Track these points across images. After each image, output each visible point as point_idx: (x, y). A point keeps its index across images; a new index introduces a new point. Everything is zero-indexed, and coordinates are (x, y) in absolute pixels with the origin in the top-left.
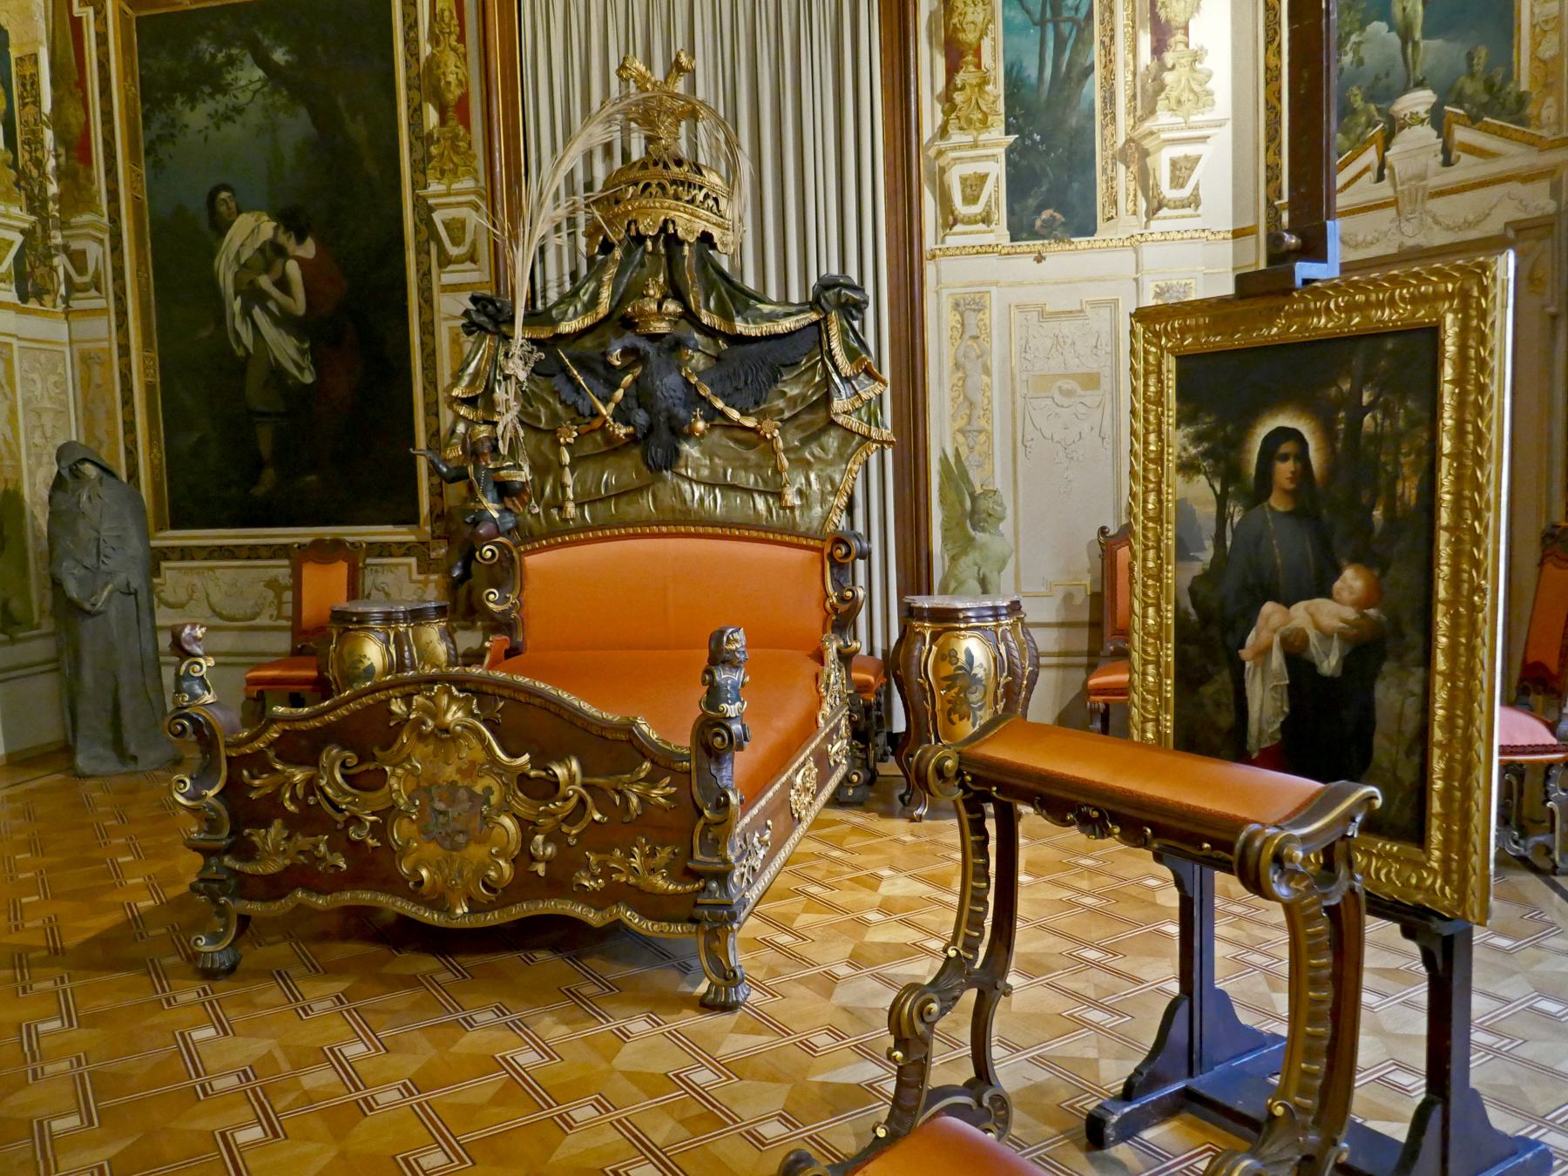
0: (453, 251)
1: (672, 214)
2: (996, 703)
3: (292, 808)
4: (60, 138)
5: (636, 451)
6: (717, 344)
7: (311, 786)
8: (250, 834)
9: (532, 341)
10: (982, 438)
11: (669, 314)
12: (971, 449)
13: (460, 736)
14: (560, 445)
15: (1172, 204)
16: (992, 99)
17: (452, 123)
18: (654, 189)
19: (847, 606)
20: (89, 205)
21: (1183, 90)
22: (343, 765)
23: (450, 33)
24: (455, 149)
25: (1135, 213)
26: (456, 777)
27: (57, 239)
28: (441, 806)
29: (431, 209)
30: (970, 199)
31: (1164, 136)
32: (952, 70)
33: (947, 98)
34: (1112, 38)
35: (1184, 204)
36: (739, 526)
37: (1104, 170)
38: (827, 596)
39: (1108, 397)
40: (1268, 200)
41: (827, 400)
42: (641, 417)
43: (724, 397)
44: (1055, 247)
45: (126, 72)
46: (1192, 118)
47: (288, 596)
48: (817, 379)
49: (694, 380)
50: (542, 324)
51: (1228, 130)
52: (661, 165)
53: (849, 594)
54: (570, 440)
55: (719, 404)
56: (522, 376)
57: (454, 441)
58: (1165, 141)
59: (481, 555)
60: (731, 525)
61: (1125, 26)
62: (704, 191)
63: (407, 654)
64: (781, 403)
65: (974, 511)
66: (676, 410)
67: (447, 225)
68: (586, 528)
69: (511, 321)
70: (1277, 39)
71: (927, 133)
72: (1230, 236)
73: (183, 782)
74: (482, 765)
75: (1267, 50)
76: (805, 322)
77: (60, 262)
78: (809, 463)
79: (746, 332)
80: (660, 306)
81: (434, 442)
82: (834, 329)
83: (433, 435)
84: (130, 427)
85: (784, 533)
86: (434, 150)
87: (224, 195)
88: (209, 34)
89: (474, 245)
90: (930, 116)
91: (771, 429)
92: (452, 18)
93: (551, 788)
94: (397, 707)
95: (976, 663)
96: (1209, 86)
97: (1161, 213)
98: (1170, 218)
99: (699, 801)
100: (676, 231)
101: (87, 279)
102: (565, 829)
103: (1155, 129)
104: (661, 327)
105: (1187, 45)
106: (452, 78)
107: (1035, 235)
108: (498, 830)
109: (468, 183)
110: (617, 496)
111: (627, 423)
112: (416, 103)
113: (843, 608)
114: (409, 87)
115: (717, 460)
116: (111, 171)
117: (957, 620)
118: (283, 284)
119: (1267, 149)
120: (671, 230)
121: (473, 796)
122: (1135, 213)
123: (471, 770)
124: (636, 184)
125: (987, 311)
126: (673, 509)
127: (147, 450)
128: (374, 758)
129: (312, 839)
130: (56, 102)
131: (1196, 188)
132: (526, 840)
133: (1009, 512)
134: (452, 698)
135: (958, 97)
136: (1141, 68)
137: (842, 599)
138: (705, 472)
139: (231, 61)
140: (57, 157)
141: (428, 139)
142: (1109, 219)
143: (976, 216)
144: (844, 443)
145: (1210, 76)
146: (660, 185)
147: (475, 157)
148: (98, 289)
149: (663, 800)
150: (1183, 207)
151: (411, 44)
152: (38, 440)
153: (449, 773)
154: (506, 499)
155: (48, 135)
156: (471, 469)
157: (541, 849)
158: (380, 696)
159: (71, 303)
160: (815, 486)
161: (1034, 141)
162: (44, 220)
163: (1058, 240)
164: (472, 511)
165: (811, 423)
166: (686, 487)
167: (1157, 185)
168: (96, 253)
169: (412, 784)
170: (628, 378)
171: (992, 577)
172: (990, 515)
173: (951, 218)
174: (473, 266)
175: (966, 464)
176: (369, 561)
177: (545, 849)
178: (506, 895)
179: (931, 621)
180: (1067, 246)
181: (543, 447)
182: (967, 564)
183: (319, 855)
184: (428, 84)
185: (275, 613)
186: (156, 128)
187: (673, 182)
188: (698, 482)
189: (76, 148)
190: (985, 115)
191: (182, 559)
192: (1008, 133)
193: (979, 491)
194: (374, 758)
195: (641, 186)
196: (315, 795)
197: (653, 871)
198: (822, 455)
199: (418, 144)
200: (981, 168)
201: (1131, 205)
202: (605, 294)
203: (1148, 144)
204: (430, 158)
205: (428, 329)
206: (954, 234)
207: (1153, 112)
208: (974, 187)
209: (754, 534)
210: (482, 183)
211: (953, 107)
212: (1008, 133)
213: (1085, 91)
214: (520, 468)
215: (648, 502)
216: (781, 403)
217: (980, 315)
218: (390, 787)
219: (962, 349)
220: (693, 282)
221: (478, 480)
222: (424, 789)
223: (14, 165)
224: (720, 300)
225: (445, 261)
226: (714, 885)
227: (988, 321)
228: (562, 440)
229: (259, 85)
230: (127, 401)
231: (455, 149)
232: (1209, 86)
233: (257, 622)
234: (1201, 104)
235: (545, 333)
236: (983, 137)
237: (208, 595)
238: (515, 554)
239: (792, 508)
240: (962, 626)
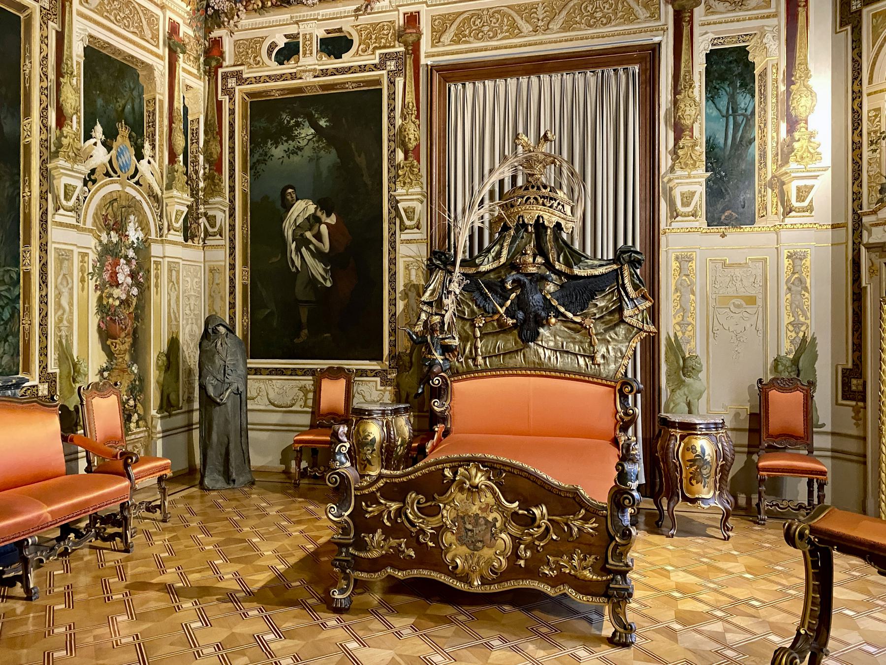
0: (408, 223)
1: (541, 213)
2: (716, 475)
3: (388, 524)
4: (207, 160)
5: (516, 332)
6: (561, 279)
7: (399, 512)
8: (364, 537)
9: (463, 274)
10: (690, 328)
11: (538, 264)
12: (684, 333)
13: (482, 490)
14: (475, 327)
15: (797, 210)
16: (699, 153)
17: (411, 159)
18: (532, 200)
19: (629, 418)
20: (220, 193)
21: (804, 152)
22: (418, 503)
23: (412, 114)
24: (412, 172)
25: (776, 214)
26: (479, 512)
27: (202, 210)
28: (470, 527)
29: (397, 202)
30: (685, 204)
31: (793, 175)
32: (677, 139)
33: (675, 152)
34: (765, 125)
35: (804, 210)
36: (569, 372)
37: (760, 192)
38: (617, 412)
39: (761, 309)
40: (854, 210)
41: (620, 310)
42: (521, 315)
43: (563, 306)
45: (244, 127)
46: (809, 166)
47: (311, 395)
48: (615, 298)
49: (549, 297)
50: (470, 266)
52: (536, 188)
53: (631, 411)
54: (481, 325)
55: (562, 310)
56: (458, 291)
57: (419, 323)
59: (433, 382)
60: (565, 372)
61: (772, 119)
62: (558, 201)
63: (392, 432)
64: (594, 310)
65: (684, 367)
66: (539, 312)
67: (405, 211)
68: (486, 370)
69: (454, 264)
70: (860, 128)
71: (663, 170)
72: (830, 227)
73: (333, 507)
74: (493, 506)
75: (853, 133)
76: (610, 270)
77: (203, 220)
78: (609, 342)
79: (579, 274)
80: (534, 260)
81: (393, 319)
82: (626, 274)
83: (392, 315)
84: (232, 306)
85: (594, 378)
86: (400, 172)
87: (290, 190)
88: (287, 111)
89: (419, 220)
90: (665, 161)
91: (588, 322)
92: (413, 106)
93: (531, 521)
94: (448, 473)
95: (706, 454)
97: (791, 214)
98: (796, 217)
99: (613, 533)
100: (544, 222)
101: (216, 230)
102: (537, 543)
103: (788, 171)
104: (532, 270)
105: (807, 129)
106: (411, 136)
107: (721, 224)
108: (500, 541)
109: (418, 189)
110: (504, 354)
111: (512, 318)
112: (392, 149)
113: (626, 419)
114: (389, 141)
115: (558, 338)
116: (232, 176)
117: (695, 429)
118: (318, 236)
119: (853, 183)
120: (541, 221)
121: (487, 521)
122: (776, 214)
123: (487, 508)
124: (523, 198)
125: (694, 262)
126: (534, 362)
127: (241, 316)
128: (434, 499)
129: (397, 541)
130: (206, 142)
132: (516, 548)
133: (704, 368)
134: (478, 469)
135: (680, 152)
136: (781, 140)
137: (626, 414)
138: (552, 344)
139: (298, 124)
140: (205, 168)
141: (398, 167)
142: (762, 217)
144: (629, 331)
145: (819, 145)
146: (535, 198)
147: (422, 176)
148: (221, 235)
149: (591, 531)
151: (391, 119)
152: (188, 312)
153: (475, 509)
154: (446, 354)
155: (201, 158)
156: (429, 338)
157: (523, 553)
158: (440, 466)
159: (206, 242)
160: (612, 353)
161: (721, 176)
162: (197, 201)
163: (734, 226)
164: (429, 359)
165: (611, 321)
166: (541, 350)
167: (789, 200)
168: (222, 217)
169: (454, 514)
170: (514, 295)
171: (694, 402)
172: (693, 369)
173: (675, 213)
174: (418, 231)
175: (681, 341)
176: (356, 379)
177: (526, 552)
178: (503, 577)
179: (680, 429)
181: (465, 328)
182: (679, 393)
183: (401, 550)
184: (400, 139)
185: (303, 404)
186: (256, 156)
187: (543, 197)
188: (547, 349)
189: (215, 164)
190: (695, 162)
191: (255, 374)
192: (707, 171)
193: (687, 356)
194: (434, 499)
195: (525, 199)
196: (401, 517)
197: (585, 568)
198: (616, 337)
199: (392, 169)
200: (692, 188)
202: (505, 252)
203: (784, 178)
204: (399, 176)
205: (393, 262)
207: (787, 162)
208: (687, 198)
209: (577, 377)
210: (425, 189)
211: (678, 157)
212: (707, 171)
213: (750, 150)
214: (454, 338)
215: (520, 358)
216: (594, 310)
217: (690, 264)
218: (442, 515)
219: (680, 282)
220: (552, 248)
221: (433, 344)
222: (461, 518)
223: (186, 174)
224: (565, 257)
225: (403, 228)
226: (619, 577)
227: (694, 267)
228: (477, 325)
229: (311, 137)
230: (232, 292)
231: (412, 172)
233: (293, 408)
234: (814, 159)
235: (472, 271)
237: (267, 394)
238: (449, 382)
239: (599, 365)
240: (699, 433)
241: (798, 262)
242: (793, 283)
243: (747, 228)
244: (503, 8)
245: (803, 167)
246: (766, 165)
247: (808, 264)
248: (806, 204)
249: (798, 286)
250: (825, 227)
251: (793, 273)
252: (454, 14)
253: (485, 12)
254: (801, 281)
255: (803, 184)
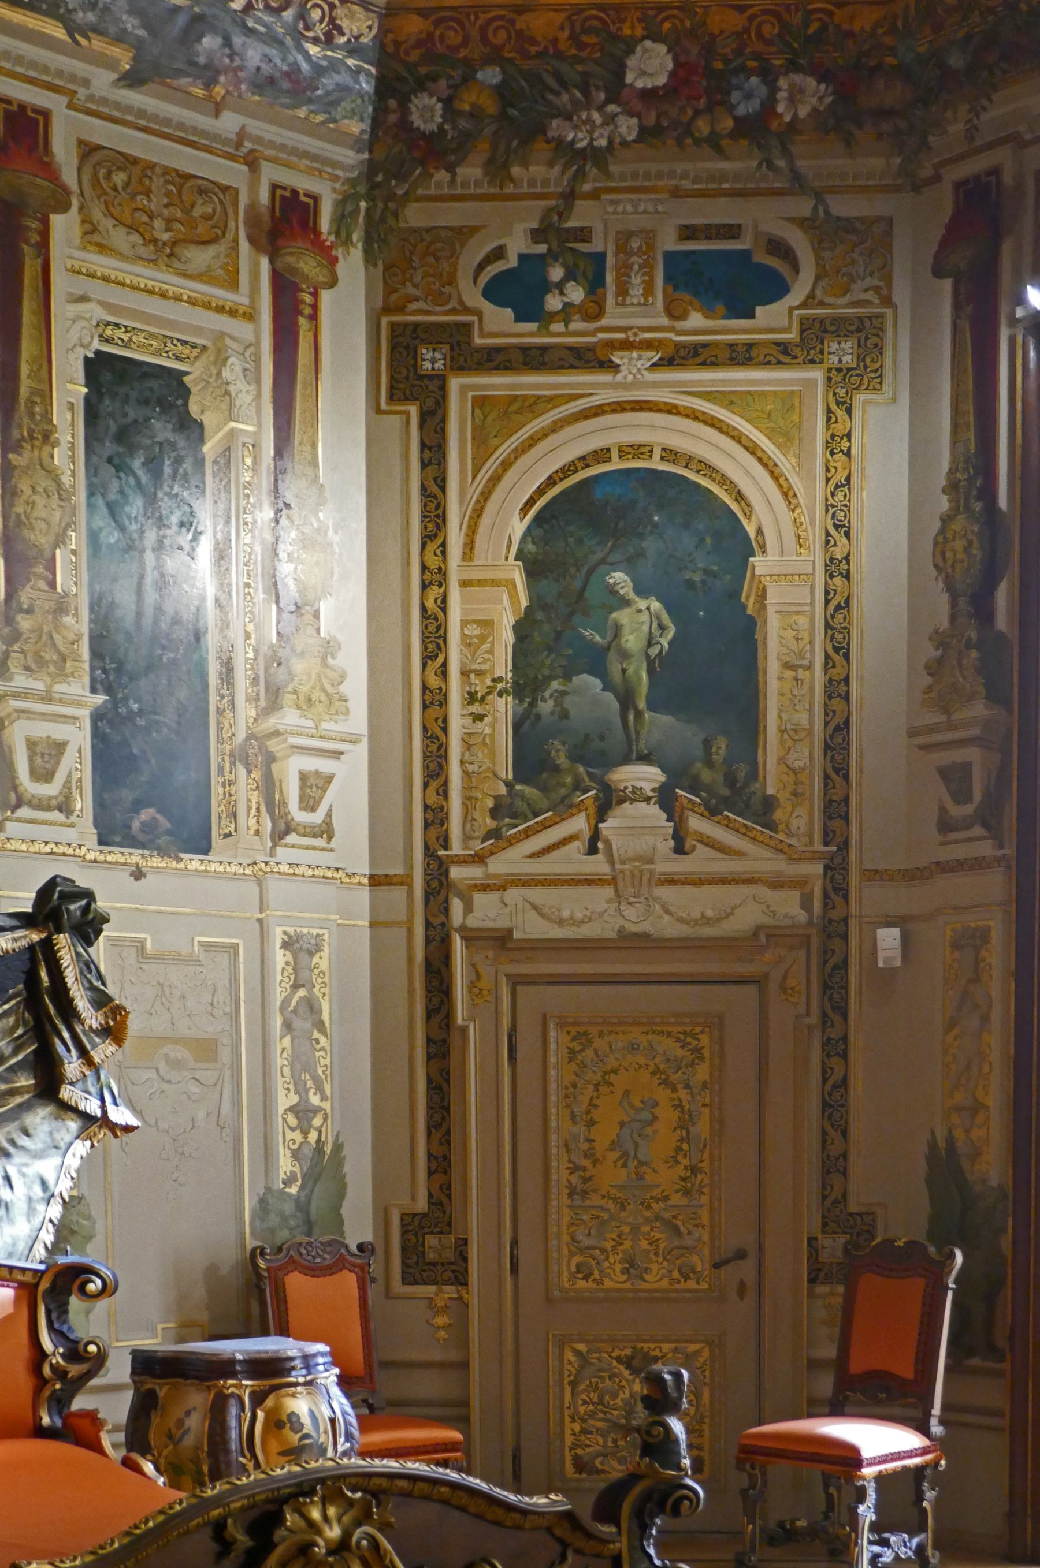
21: (314, 688)
25: (257, 833)
30: (44, 775)
31: (293, 740)
37: (221, 770)
39: (227, 1073)
44: (157, 862)
51: (362, 750)
58: (293, 747)
72: (366, 881)
96: (343, 688)
103: (281, 728)
107: (131, 842)
131: (329, 814)
142: (228, 835)
143: (50, 798)
145: (343, 677)
150: (314, 836)
167: (284, 803)
180: (174, 864)
192: (93, 690)
200: (59, 731)
201: (252, 822)
203: (273, 745)
206: (19, 820)
212: (93, 690)
232: (343, 688)
234: (333, 711)
236: (59, 688)
241: (303, 957)
242: (295, 1011)
243: (193, 862)
245: (310, 723)
246: (232, 703)
247: (324, 965)
248: (316, 818)
249: (306, 1019)
250: (356, 880)
251: (296, 987)
254: (311, 1006)
255: (313, 769)
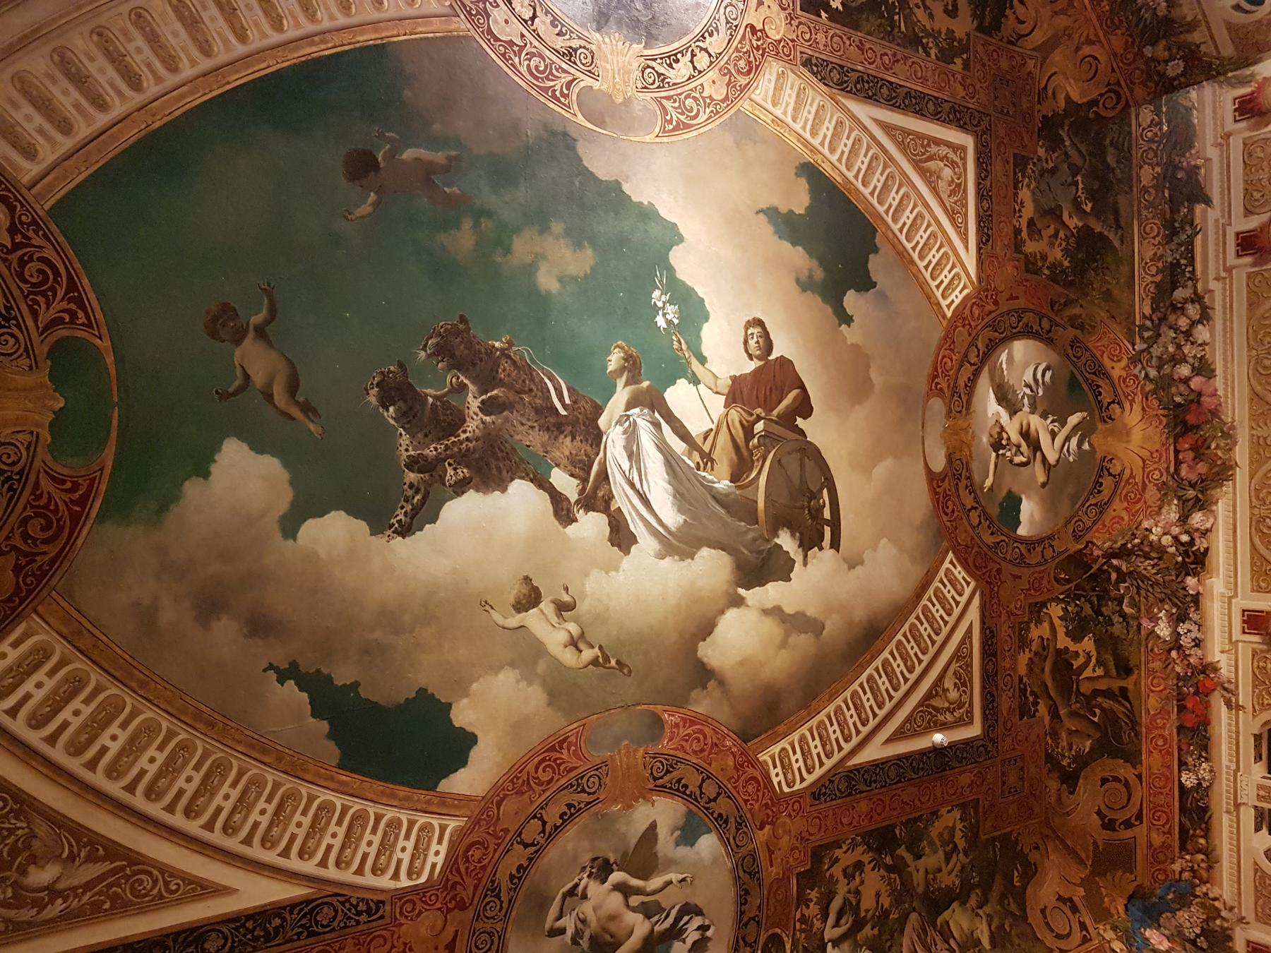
244: (1252, 486)
252: (1252, 558)
253: (1256, 511)
